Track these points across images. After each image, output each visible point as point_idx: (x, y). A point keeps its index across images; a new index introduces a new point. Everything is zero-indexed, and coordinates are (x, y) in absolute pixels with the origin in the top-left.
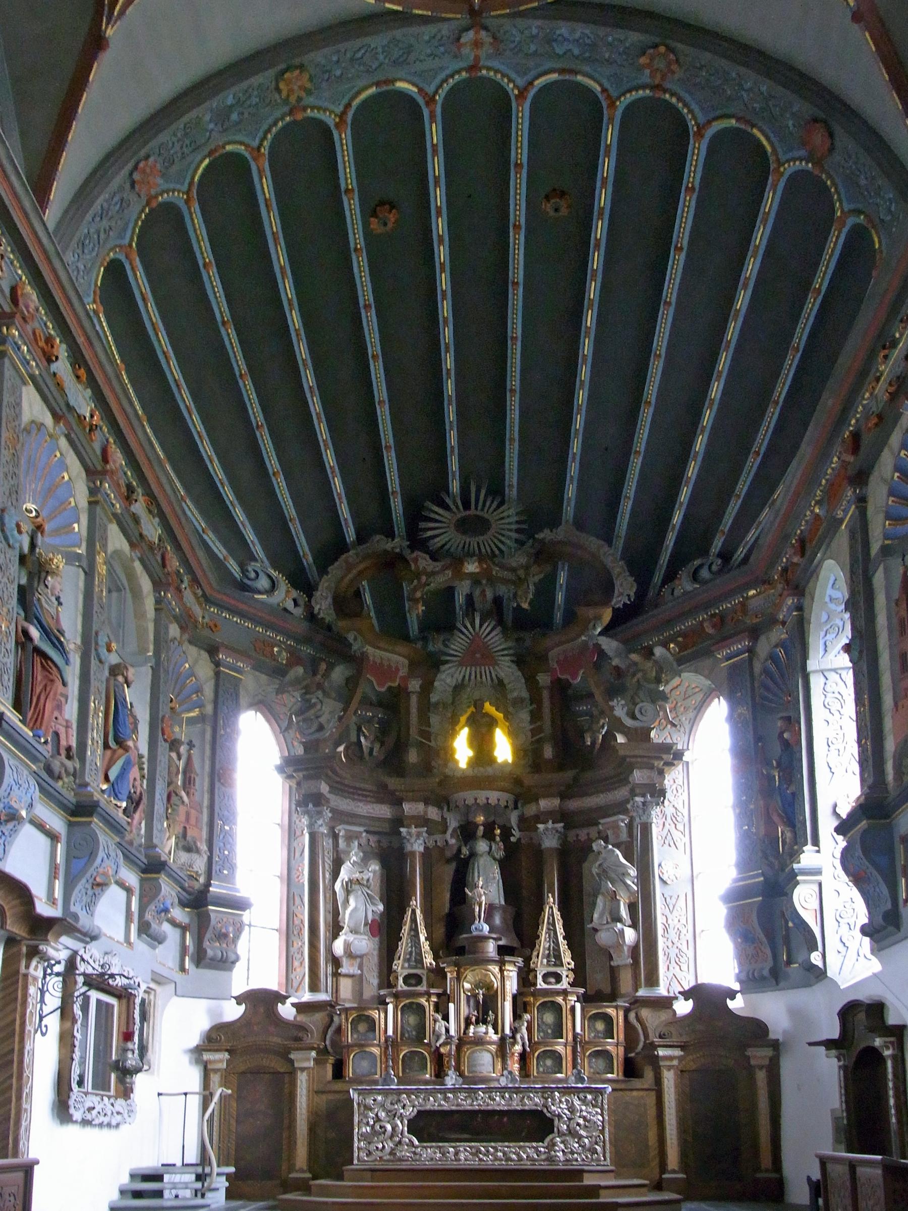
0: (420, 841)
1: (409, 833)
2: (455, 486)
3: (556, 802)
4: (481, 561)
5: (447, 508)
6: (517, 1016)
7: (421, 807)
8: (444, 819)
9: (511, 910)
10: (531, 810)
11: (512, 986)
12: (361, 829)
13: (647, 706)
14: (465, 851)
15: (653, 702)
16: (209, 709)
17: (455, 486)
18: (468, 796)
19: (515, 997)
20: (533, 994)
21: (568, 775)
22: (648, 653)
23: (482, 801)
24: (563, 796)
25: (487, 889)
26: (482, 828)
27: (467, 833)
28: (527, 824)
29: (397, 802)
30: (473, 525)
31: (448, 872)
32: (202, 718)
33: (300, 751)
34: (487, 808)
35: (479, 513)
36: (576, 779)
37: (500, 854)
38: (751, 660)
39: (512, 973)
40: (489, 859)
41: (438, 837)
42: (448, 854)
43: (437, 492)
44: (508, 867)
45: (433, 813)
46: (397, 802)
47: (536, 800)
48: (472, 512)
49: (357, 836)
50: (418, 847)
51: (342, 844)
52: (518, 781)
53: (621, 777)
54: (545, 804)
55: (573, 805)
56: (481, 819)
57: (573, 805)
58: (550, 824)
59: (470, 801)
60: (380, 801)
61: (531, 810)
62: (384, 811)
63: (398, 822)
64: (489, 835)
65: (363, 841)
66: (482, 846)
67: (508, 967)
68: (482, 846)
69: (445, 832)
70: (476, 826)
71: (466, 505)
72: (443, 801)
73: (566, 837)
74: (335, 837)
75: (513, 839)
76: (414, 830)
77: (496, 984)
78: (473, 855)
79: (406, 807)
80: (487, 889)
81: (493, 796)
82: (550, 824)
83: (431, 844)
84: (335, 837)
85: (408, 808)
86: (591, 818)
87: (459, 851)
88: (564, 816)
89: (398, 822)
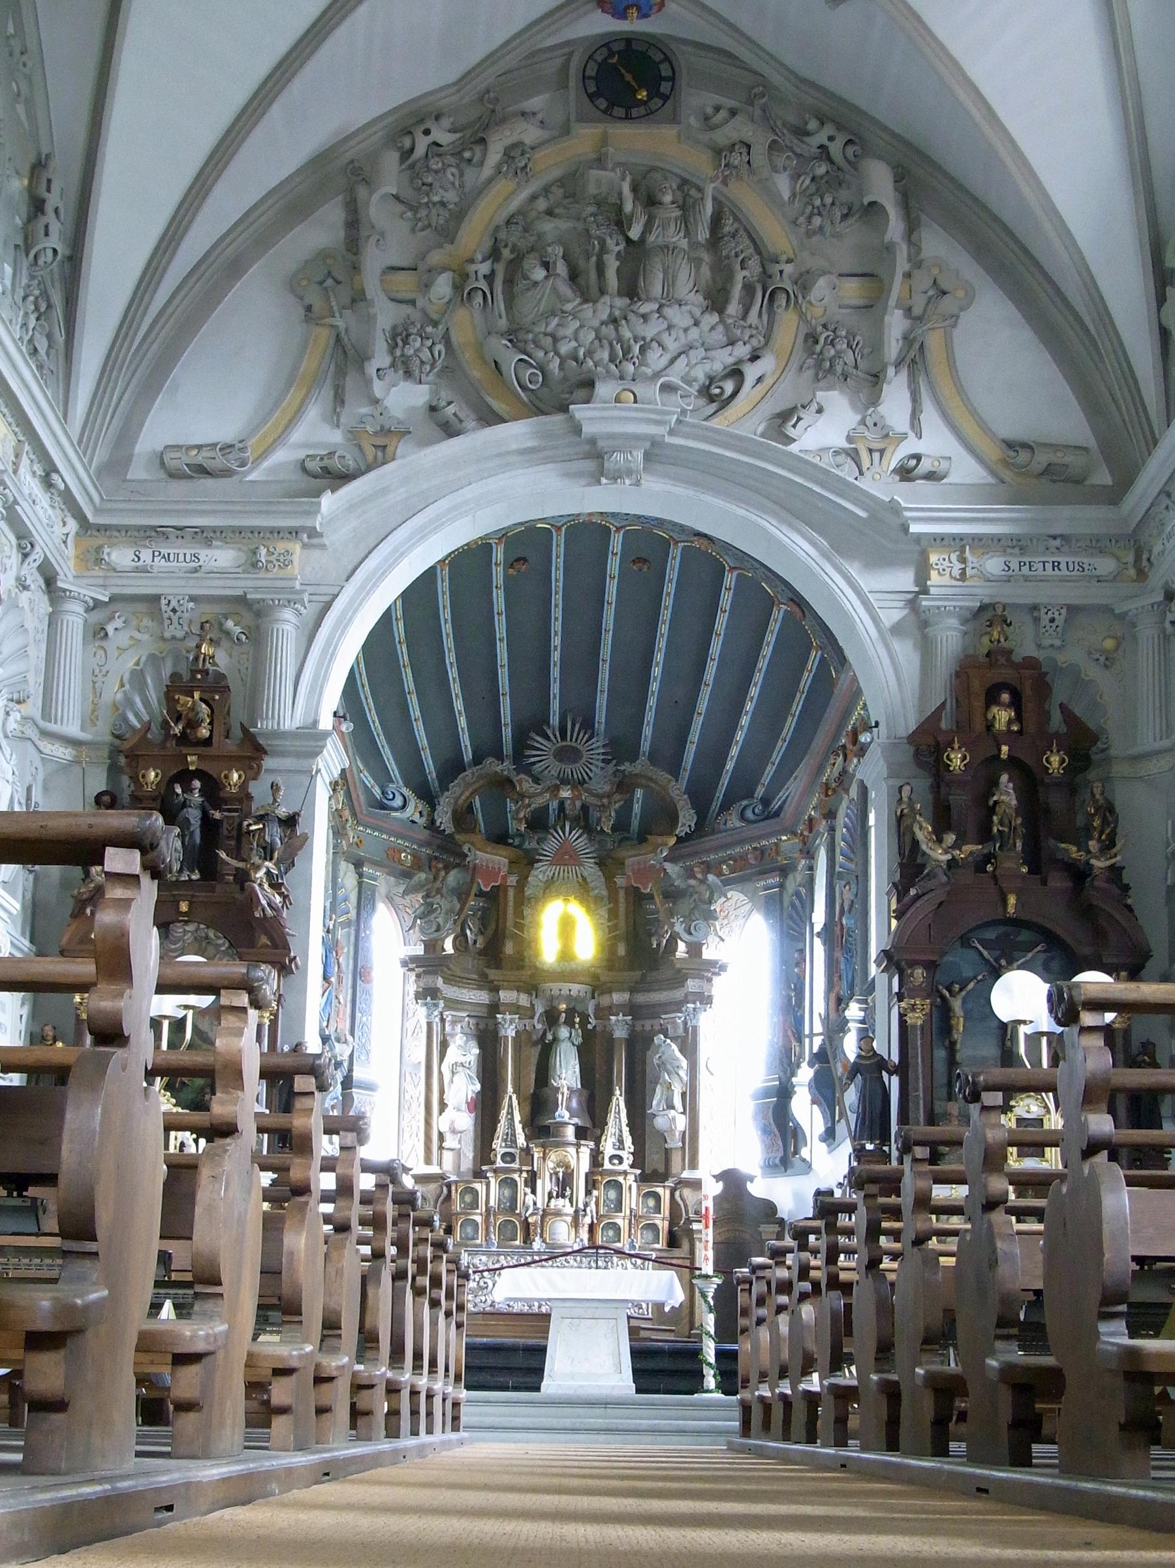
0: (513, 1027)
1: (504, 1020)
2: (555, 720)
3: (626, 996)
4: (574, 788)
5: (548, 738)
6: (588, 1193)
7: (514, 994)
8: (533, 1005)
9: (585, 1093)
10: (605, 1000)
11: (585, 1165)
12: (465, 1014)
13: (701, 923)
14: (550, 1037)
15: (706, 919)
16: (353, 914)
17: (555, 720)
18: (554, 988)
19: (587, 1175)
20: (601, 1174)
21: (637, 974)
22: (703, 881)
23: (565, 992)
24: (632, 991)
25: (567, 1074)
26: (564, 1015)
27: (551, 1018)
28: (603, 1013)
29: (494, 989)
30: (568, 755)
31: (534, 1053)
32: (348, 924)
33: (419, 950)
34: (569, 998)
35: (573, 744)
36: (643, 978)
37: (579, 1040)
38: (781, 894)
39: (585, 1153)
40: (569, 1044)
41: (527, 1021)
42: (535, 1038)
43: (539, 724)
44: (585, 1053)
45: (524, 1000)
46: (494, 989)
47: (610, 992)
48: (569, 743)
49: (461, 1020)
50: (510, 1032)
51: (448, 1028)
52: (596, 977)
53: (679, 979)
54: (618, 998)
55: (641, 998)
56: (563, 1006)
57: (641, 998)
58: (621, 1017)
59: (555, 992)
60: (480, 988)
61: (605, 1000)
62: (483, 997)
63: (494, 1008)
64: (570, 1023)
65: (465, 1024)
66: (564, 1032)
67: (583, 1149)
68: (564, 1032)
69: (532, 1018)
70: (560, 1013)
71: (564, 737)
72: (532, 988)
73: (634, 1026)
74: (443, 1020)
75: (590, 1027)
76: (508, 1017)
77: (573, 1164)
78: (555, 1039)
79: (502, 994)
80: (567, 1074)
81: (576, 989)
82: (621, 1017)
83: (521, 1028)
84: (443, 1020)
85: (506, 996)
86: (654, 1011)
87: (544, 1034)
88: (633, 1010)
89: (494, 1008)
